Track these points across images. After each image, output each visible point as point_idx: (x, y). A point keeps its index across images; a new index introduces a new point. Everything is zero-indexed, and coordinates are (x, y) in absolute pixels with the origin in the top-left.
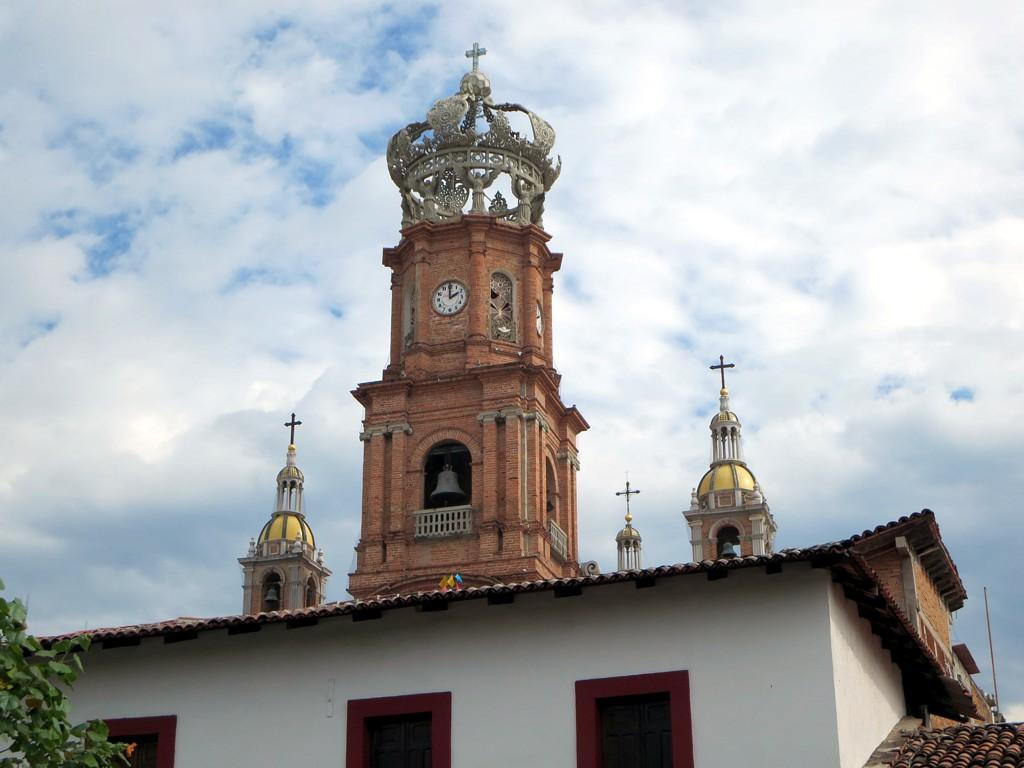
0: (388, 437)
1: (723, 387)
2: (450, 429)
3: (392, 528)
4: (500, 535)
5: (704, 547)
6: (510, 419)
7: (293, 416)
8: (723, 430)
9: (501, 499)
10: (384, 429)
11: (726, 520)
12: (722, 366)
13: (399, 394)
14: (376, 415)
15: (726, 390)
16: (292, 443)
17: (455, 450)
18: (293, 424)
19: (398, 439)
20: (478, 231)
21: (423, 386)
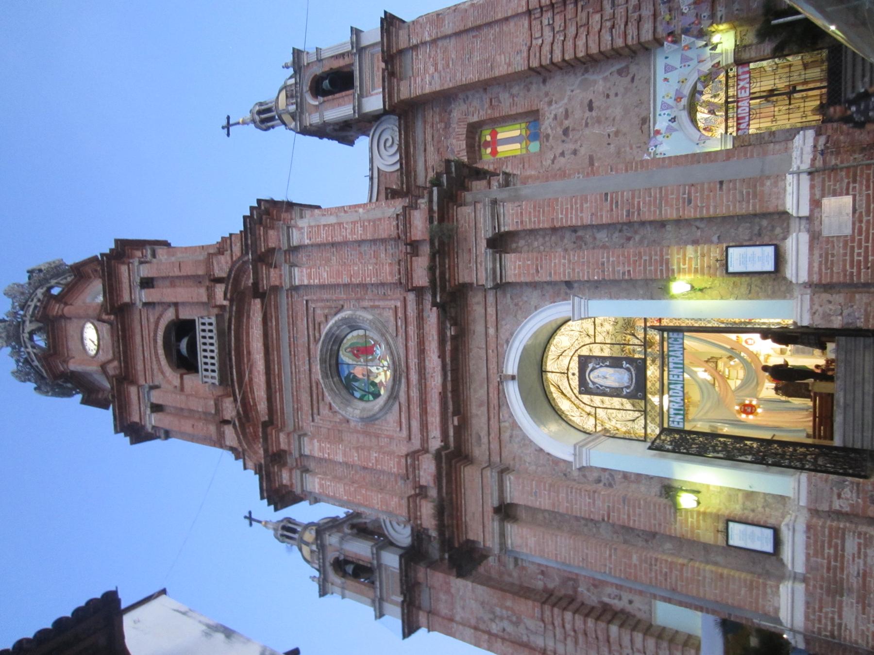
0: (157, 408)
1: (238, 123)
2: (155, 341)
3: (213, 412)
4: (219, 280)
5: (326, 110)
6: (145, 271)
7: (246, 517)
8: (265, 118)
9: (196, 280)
10: (148, 411)
11: (306, 88)
12: (228, 126)
13: (129, 393)
14: (141, 419)
15: (241, 121)
16: (259, 522)
17: (173, 338)
18: (250, 518)
19: (156, 397)
20: (53, 308)
21: (126, 367)
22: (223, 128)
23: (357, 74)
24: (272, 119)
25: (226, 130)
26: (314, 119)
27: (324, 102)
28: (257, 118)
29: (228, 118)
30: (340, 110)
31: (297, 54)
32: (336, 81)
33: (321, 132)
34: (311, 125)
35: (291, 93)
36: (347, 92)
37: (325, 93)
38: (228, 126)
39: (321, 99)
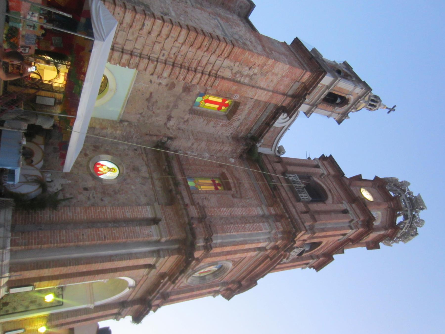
8: (374, 102)
11: (349, 105)
12: (392, 109)
22: (394, 110)
23: (322, 97)
24: (372, 101)
25: (394, 109)
26: (359, 90)
27: (347, 95)
28: (377, 105)
29: (389, 112)
30: (344, 86)
31: (339, 122)
32: (333, 100)
33: (358, 81)
34: (362, 89)
35: (355, 106)
36: (334, 92)
37: (343, 98)
38: (392, 109)
39: (347, 97)
